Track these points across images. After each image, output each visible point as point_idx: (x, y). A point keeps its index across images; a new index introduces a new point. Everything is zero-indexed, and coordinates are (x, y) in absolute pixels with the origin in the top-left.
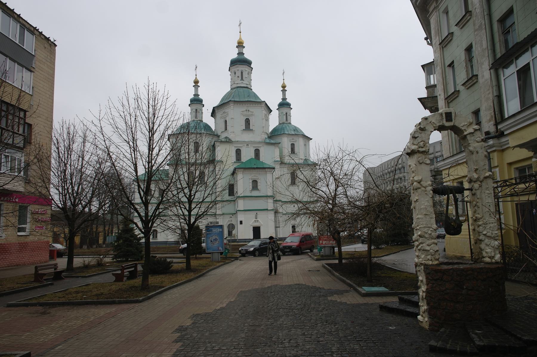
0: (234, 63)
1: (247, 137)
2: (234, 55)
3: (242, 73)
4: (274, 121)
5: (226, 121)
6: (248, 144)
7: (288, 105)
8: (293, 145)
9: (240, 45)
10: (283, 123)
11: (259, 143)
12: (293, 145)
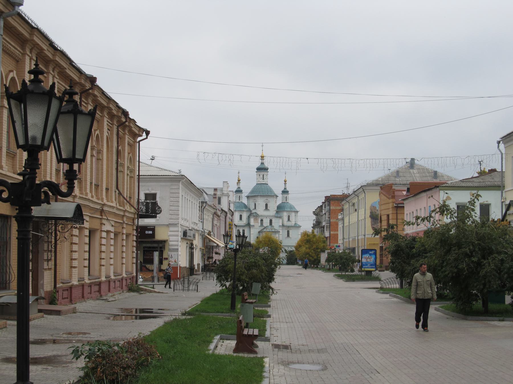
0: (259, 169)
1: (266, 213)
2: (258, 165)
3: (263, 175)
4: (279, 201)
5: (255, 204)
6: (266, 217)
7: (287, 192)
8: (289, 217)
9: (262, 157)
10: (284, 202)
11: (272, 216)
12: (289, 217)
